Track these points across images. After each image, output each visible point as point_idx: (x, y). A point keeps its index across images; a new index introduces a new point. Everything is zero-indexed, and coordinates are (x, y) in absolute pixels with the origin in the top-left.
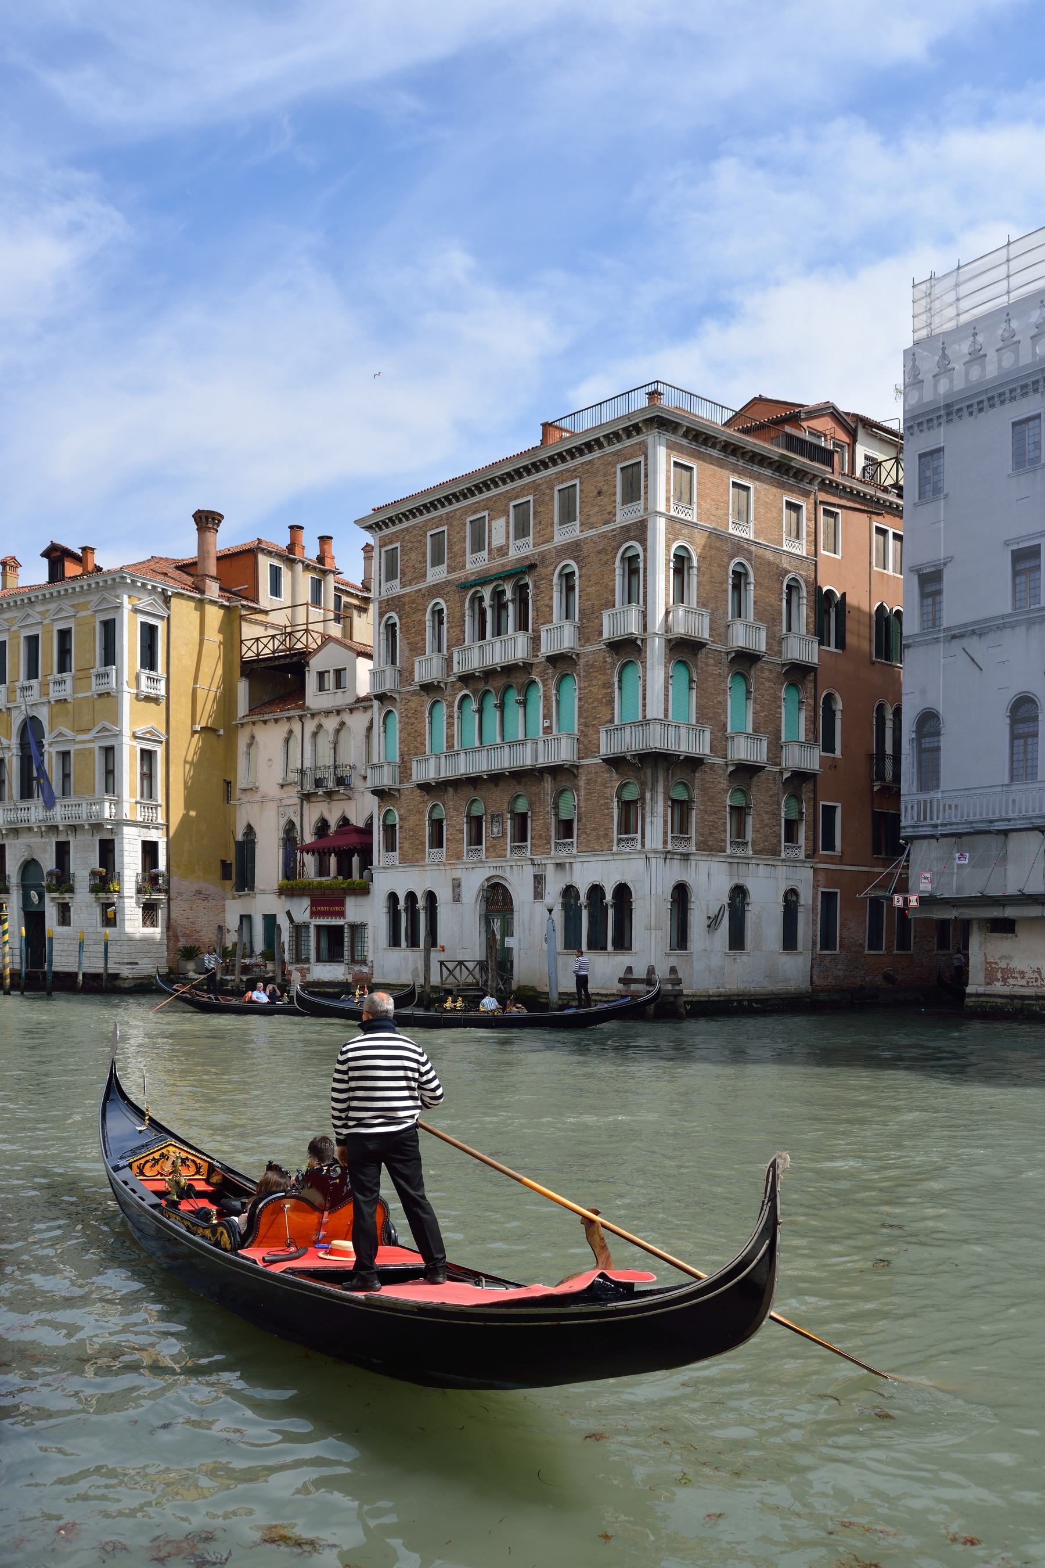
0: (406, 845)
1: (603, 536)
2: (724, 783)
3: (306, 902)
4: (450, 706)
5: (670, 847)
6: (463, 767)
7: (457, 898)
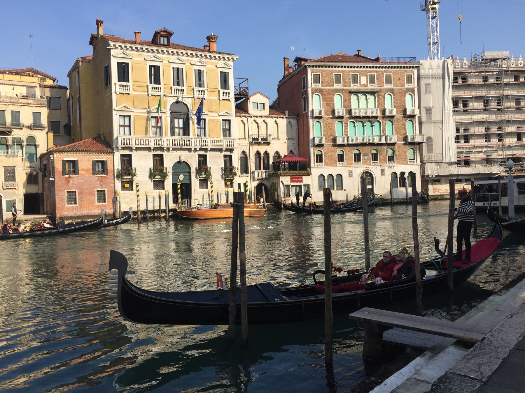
0: (327, 161)
1: (401, 89)
3: (289, 178)
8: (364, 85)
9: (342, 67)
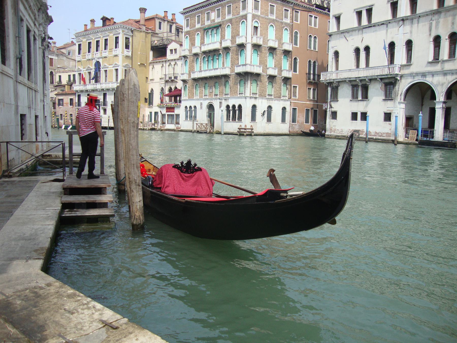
2: (266, 80)
5: (251, 96)
6: (203, 75)
7: (201, 108)
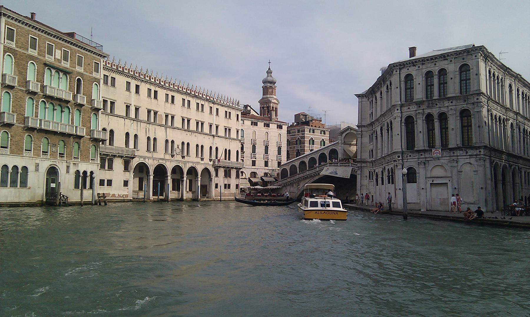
1: (90, 77)
4: (37, 102)
7: (37, 170)
8: (58, 60)
9: (40, 30)
